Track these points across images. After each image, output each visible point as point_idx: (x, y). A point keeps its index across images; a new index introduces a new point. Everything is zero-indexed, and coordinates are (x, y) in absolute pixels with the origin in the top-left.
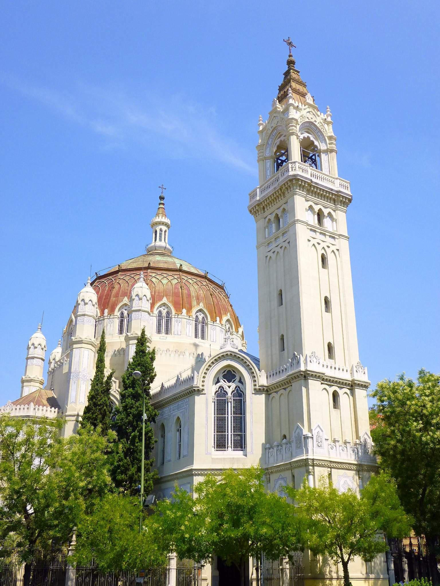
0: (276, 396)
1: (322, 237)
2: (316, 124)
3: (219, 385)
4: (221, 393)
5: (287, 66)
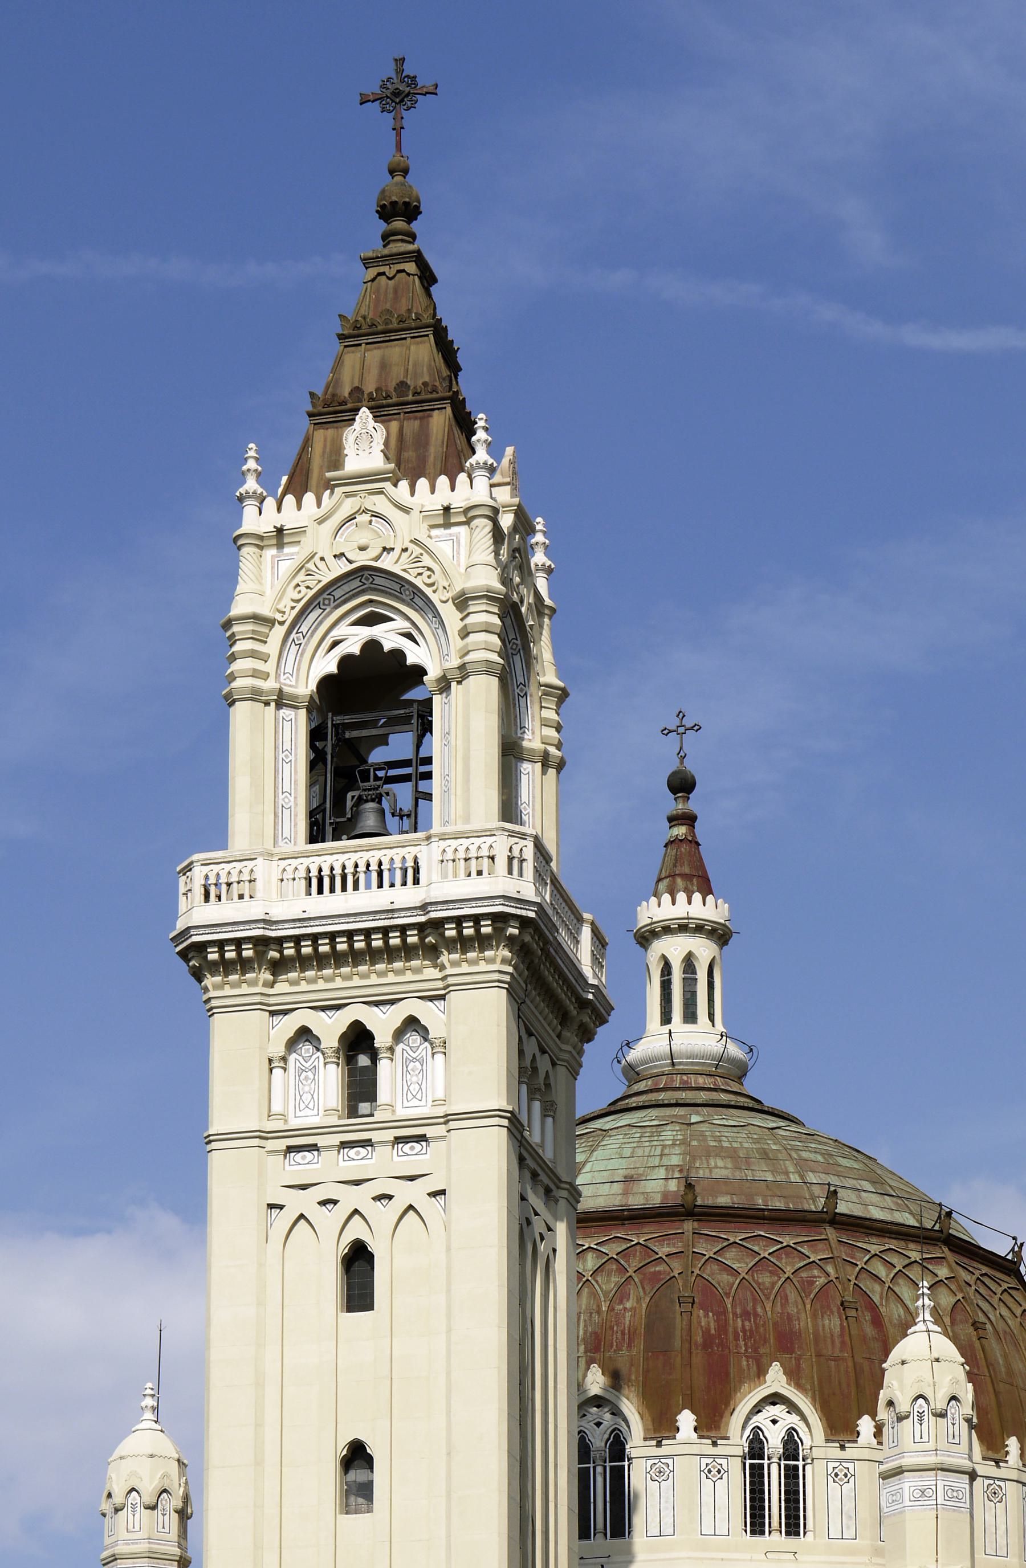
1: (355, 1163)
2: (387, 563)
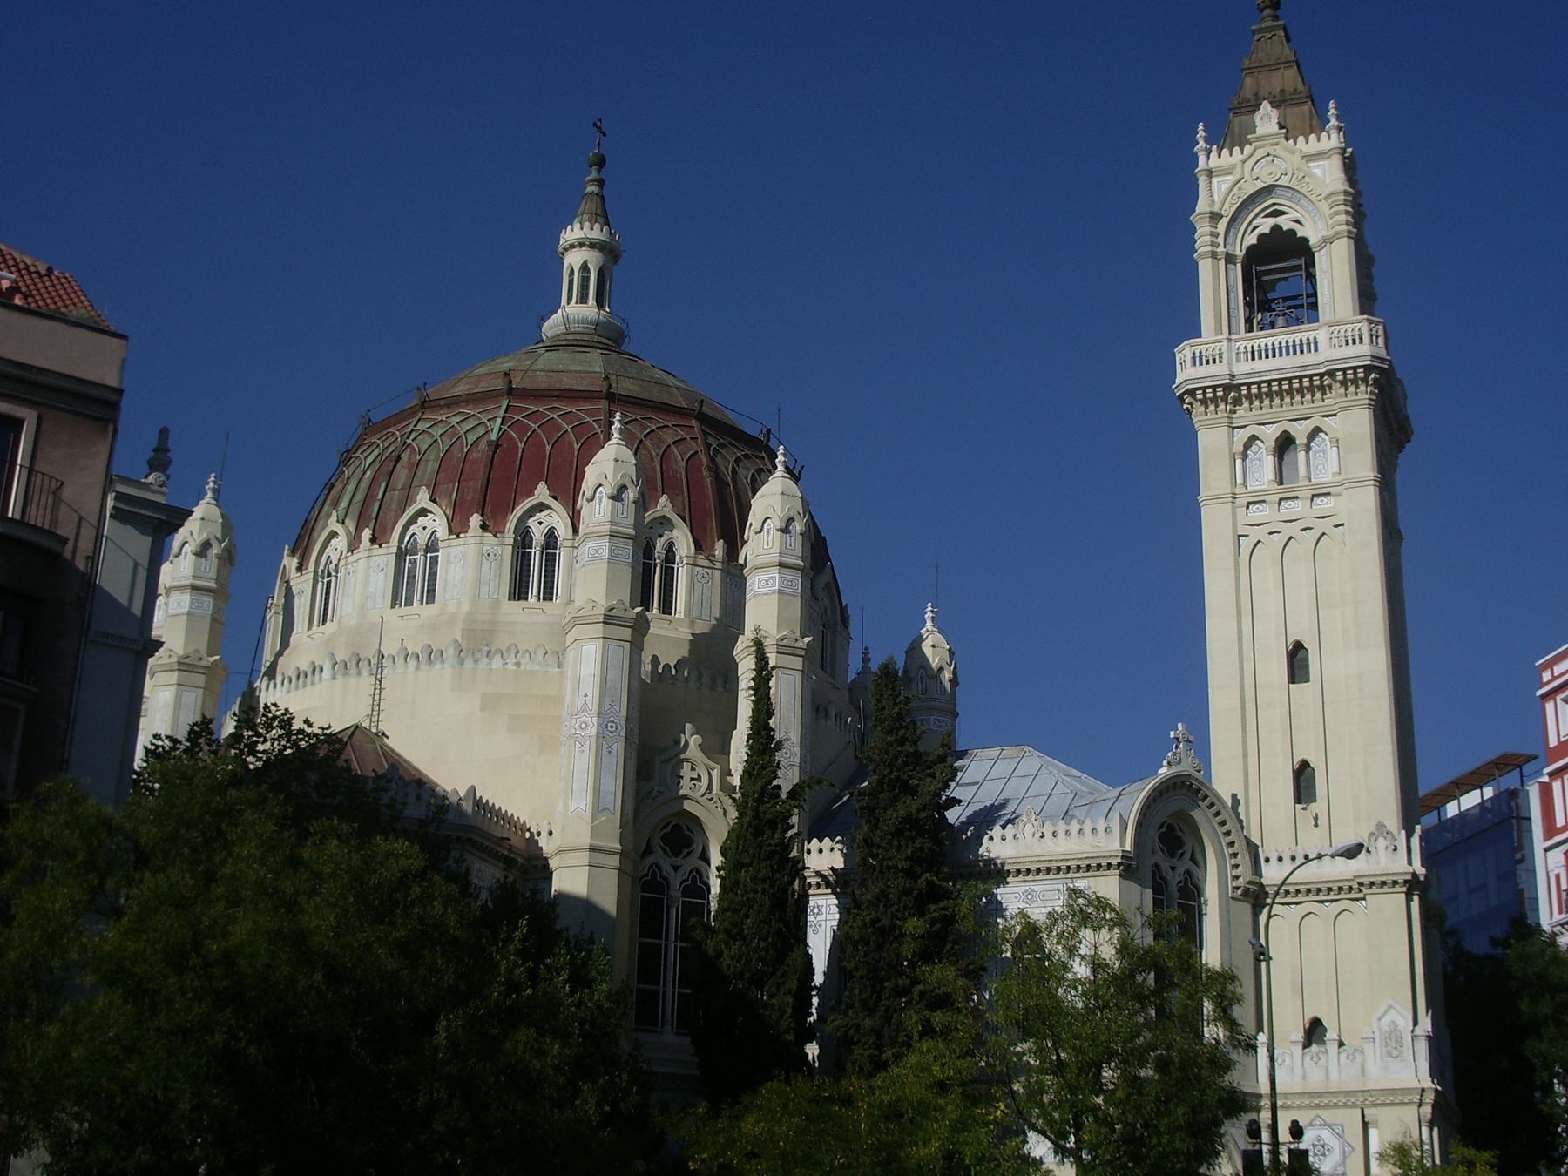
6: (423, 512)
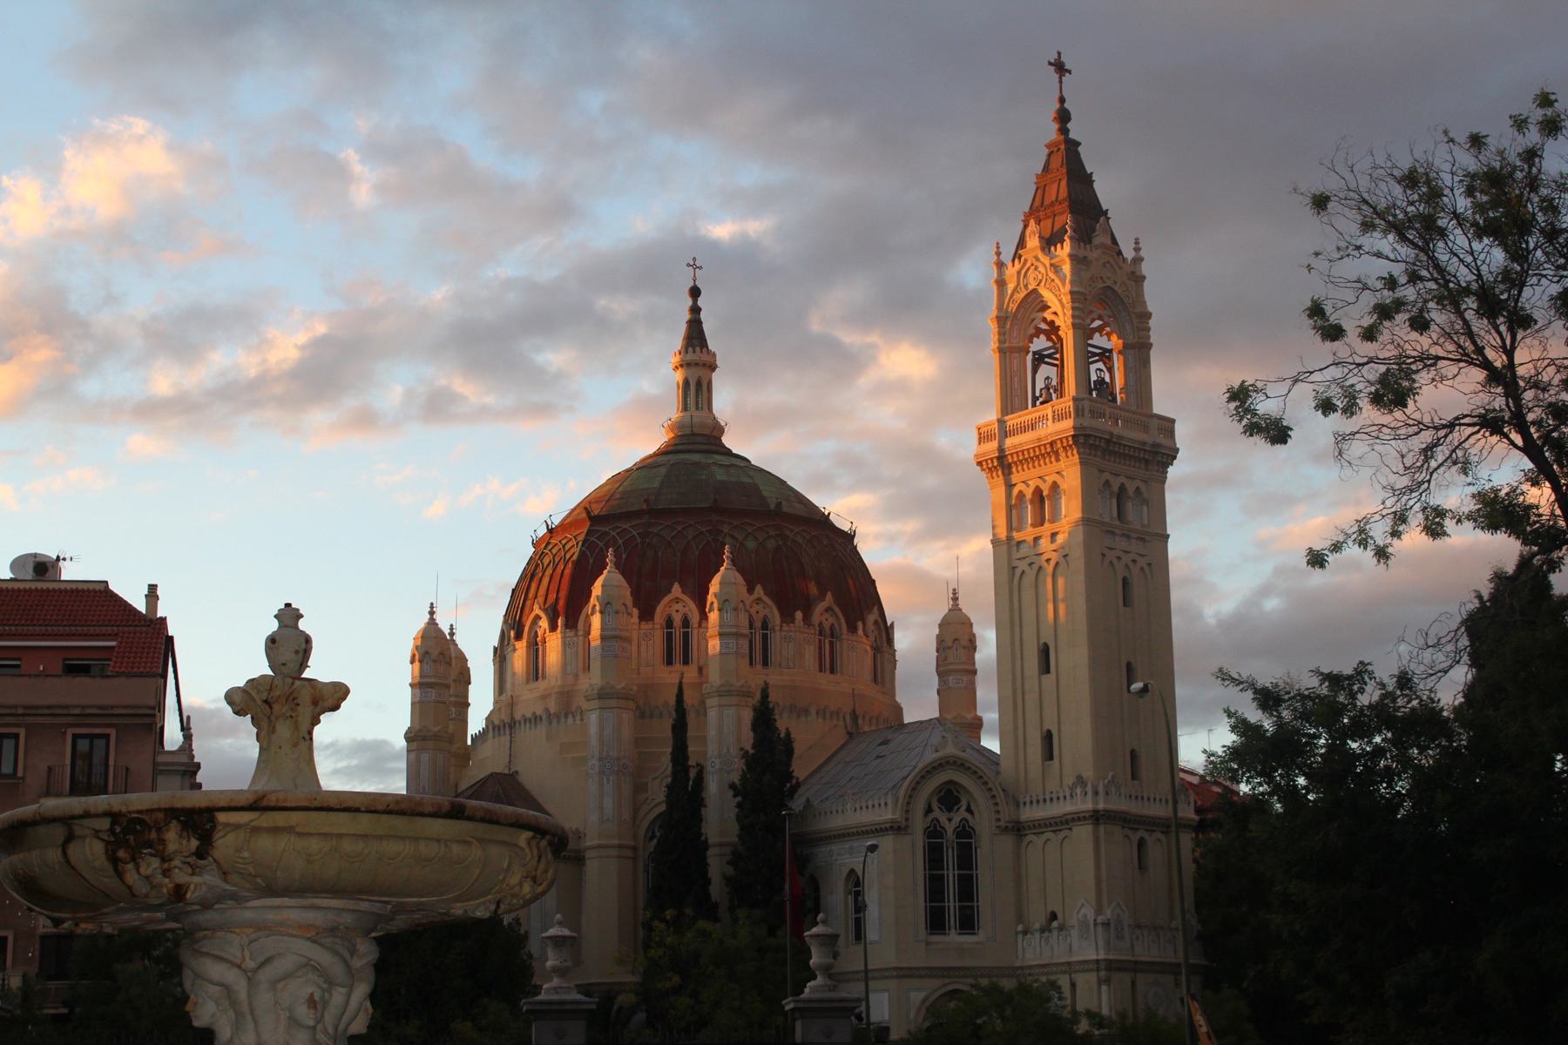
0: (1038, 841)
2: (1116, 288)
3: (931, 816)
4: (934, 832)
5: (1055, 126)
6: (538, 617)
